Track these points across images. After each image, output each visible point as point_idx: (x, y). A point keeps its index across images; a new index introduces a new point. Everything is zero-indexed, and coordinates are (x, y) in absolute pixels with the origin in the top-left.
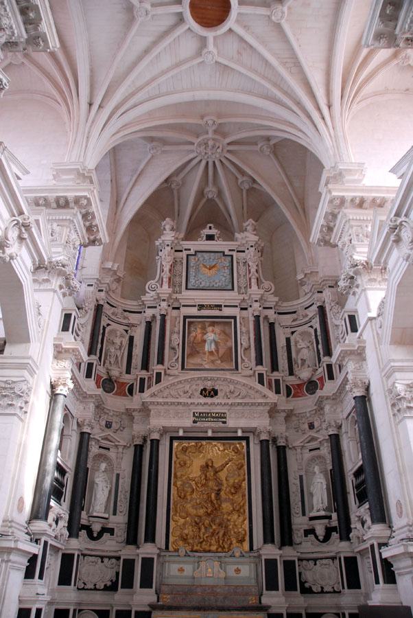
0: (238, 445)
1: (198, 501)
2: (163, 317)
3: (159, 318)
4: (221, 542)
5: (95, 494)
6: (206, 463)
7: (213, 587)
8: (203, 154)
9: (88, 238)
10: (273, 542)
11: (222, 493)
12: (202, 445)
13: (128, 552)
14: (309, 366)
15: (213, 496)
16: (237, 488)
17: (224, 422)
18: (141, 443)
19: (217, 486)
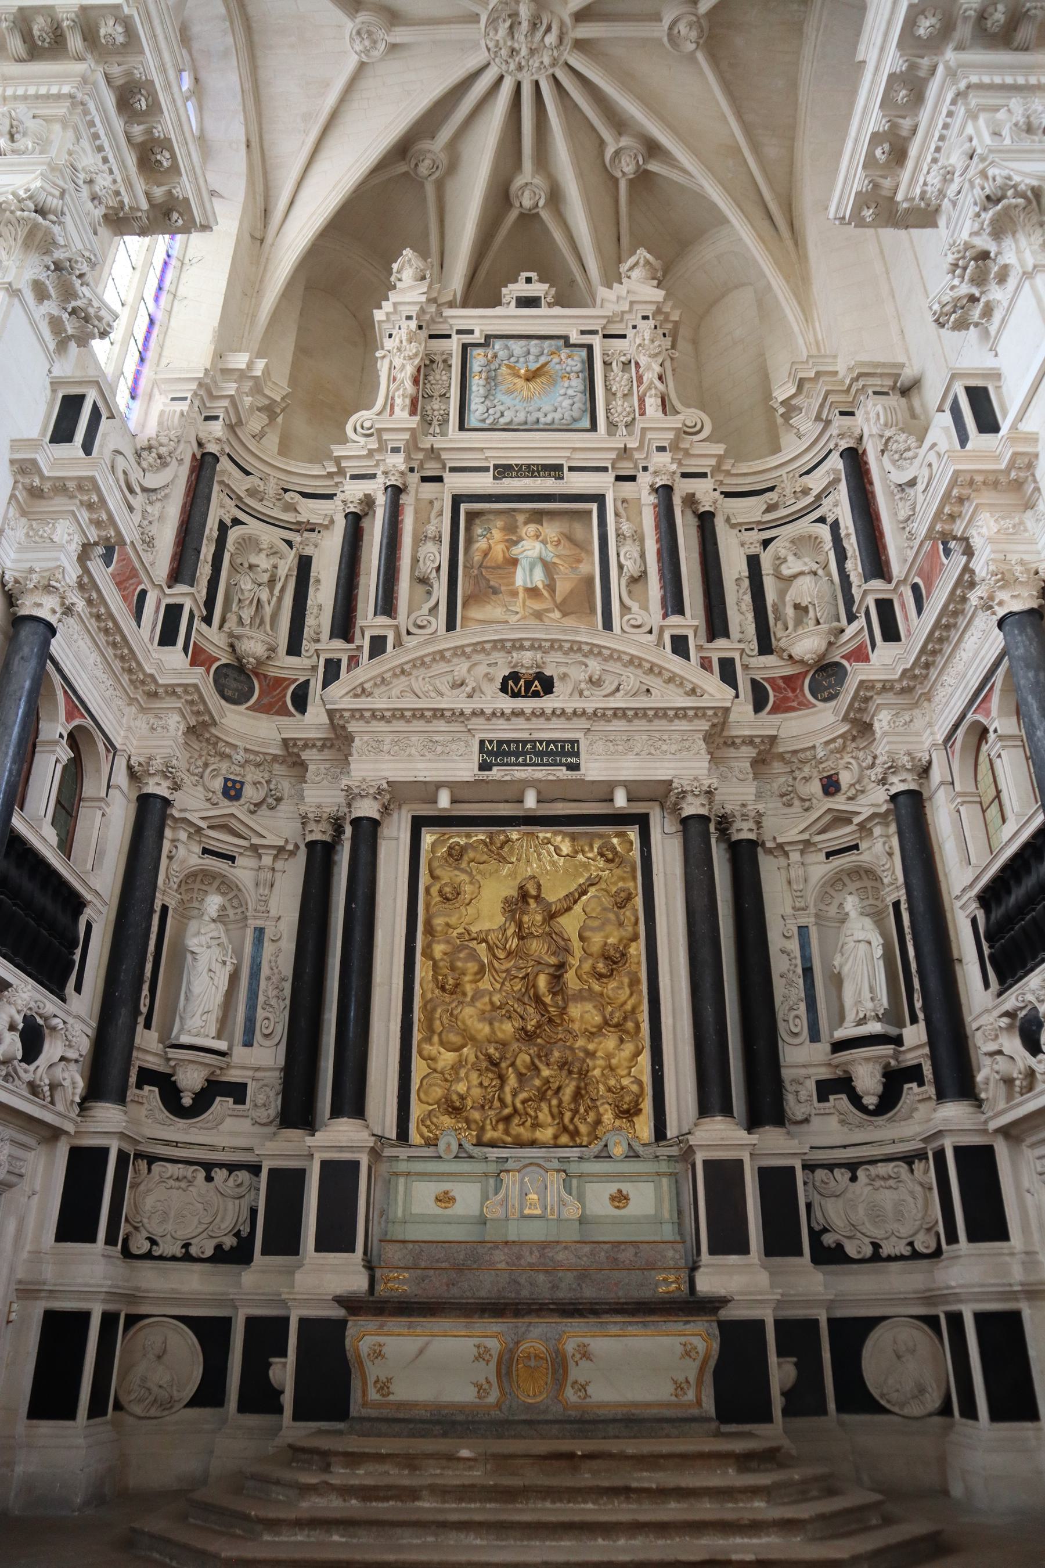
0: (615, 841)
1: (496, 999)
2: (396, 492)
3: (381, 500)
4: (568, 1115)
5: (189, 982)
6: (521, 888)
7: (544, 1246)
8: (504, 52)
9: (147, 195)
10: (727, 1110)
11: (570, 976)
12: (508, 840)
13: (283, 1148)
14: (818, 623)
15: (542, 982)
16: (614, 960)
17: (575, 767)
18: (327, 838)
19: (554, 954)
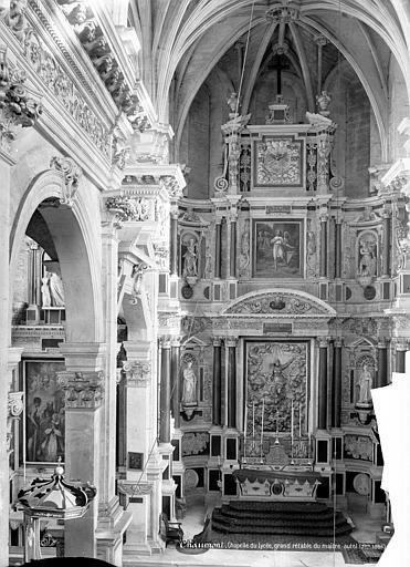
10: (325, 428)
13: (215, 431)
